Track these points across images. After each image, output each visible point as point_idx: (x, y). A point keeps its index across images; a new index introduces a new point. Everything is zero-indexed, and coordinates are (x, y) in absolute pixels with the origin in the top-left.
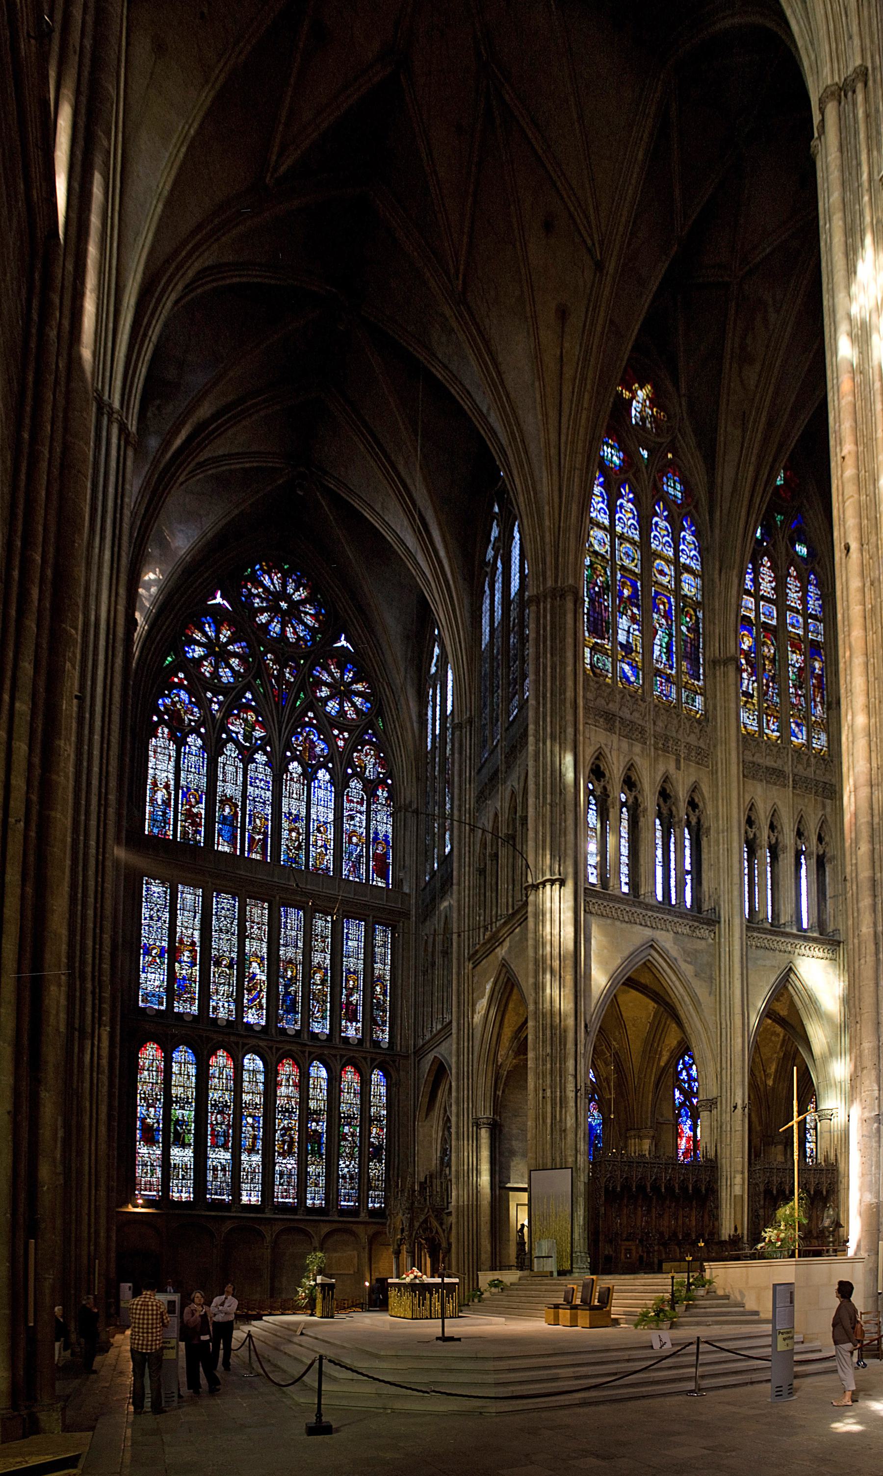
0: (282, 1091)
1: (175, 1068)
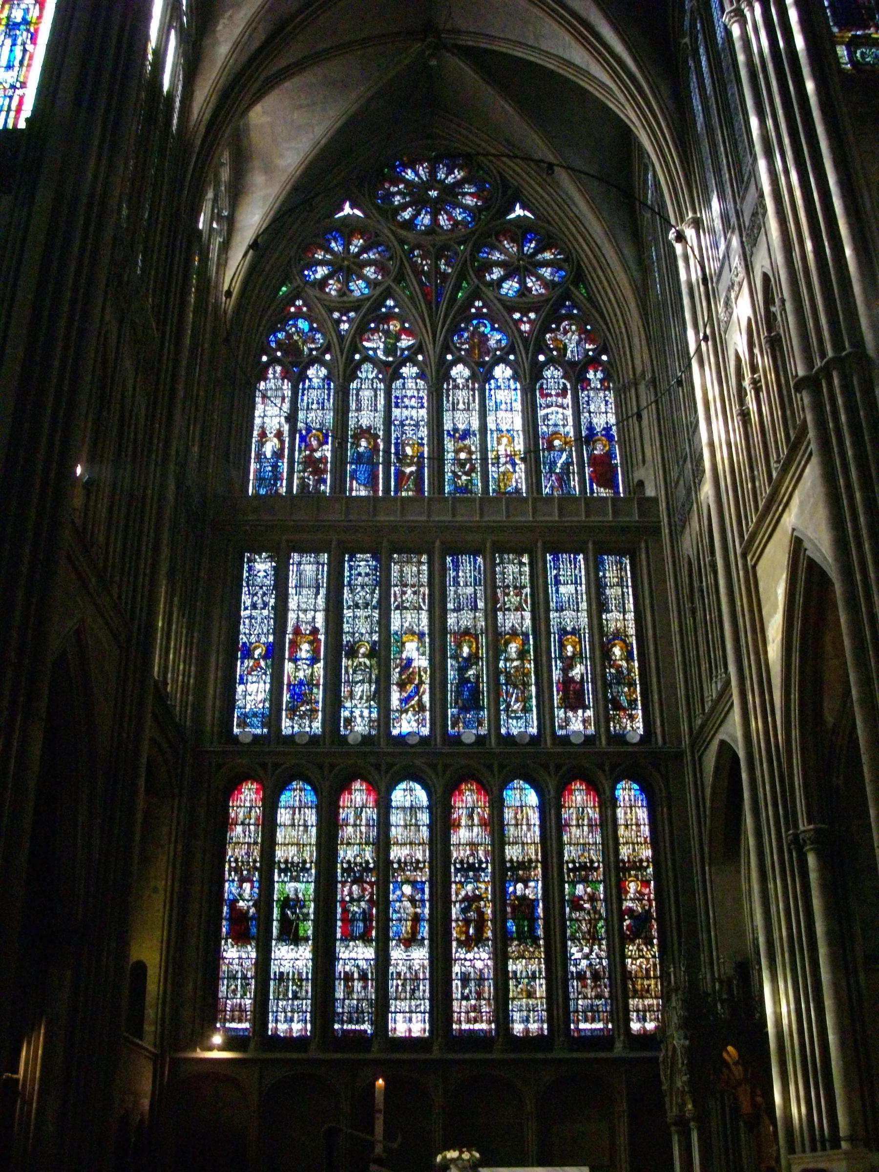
0: (462, 835)
1: (283, 816)
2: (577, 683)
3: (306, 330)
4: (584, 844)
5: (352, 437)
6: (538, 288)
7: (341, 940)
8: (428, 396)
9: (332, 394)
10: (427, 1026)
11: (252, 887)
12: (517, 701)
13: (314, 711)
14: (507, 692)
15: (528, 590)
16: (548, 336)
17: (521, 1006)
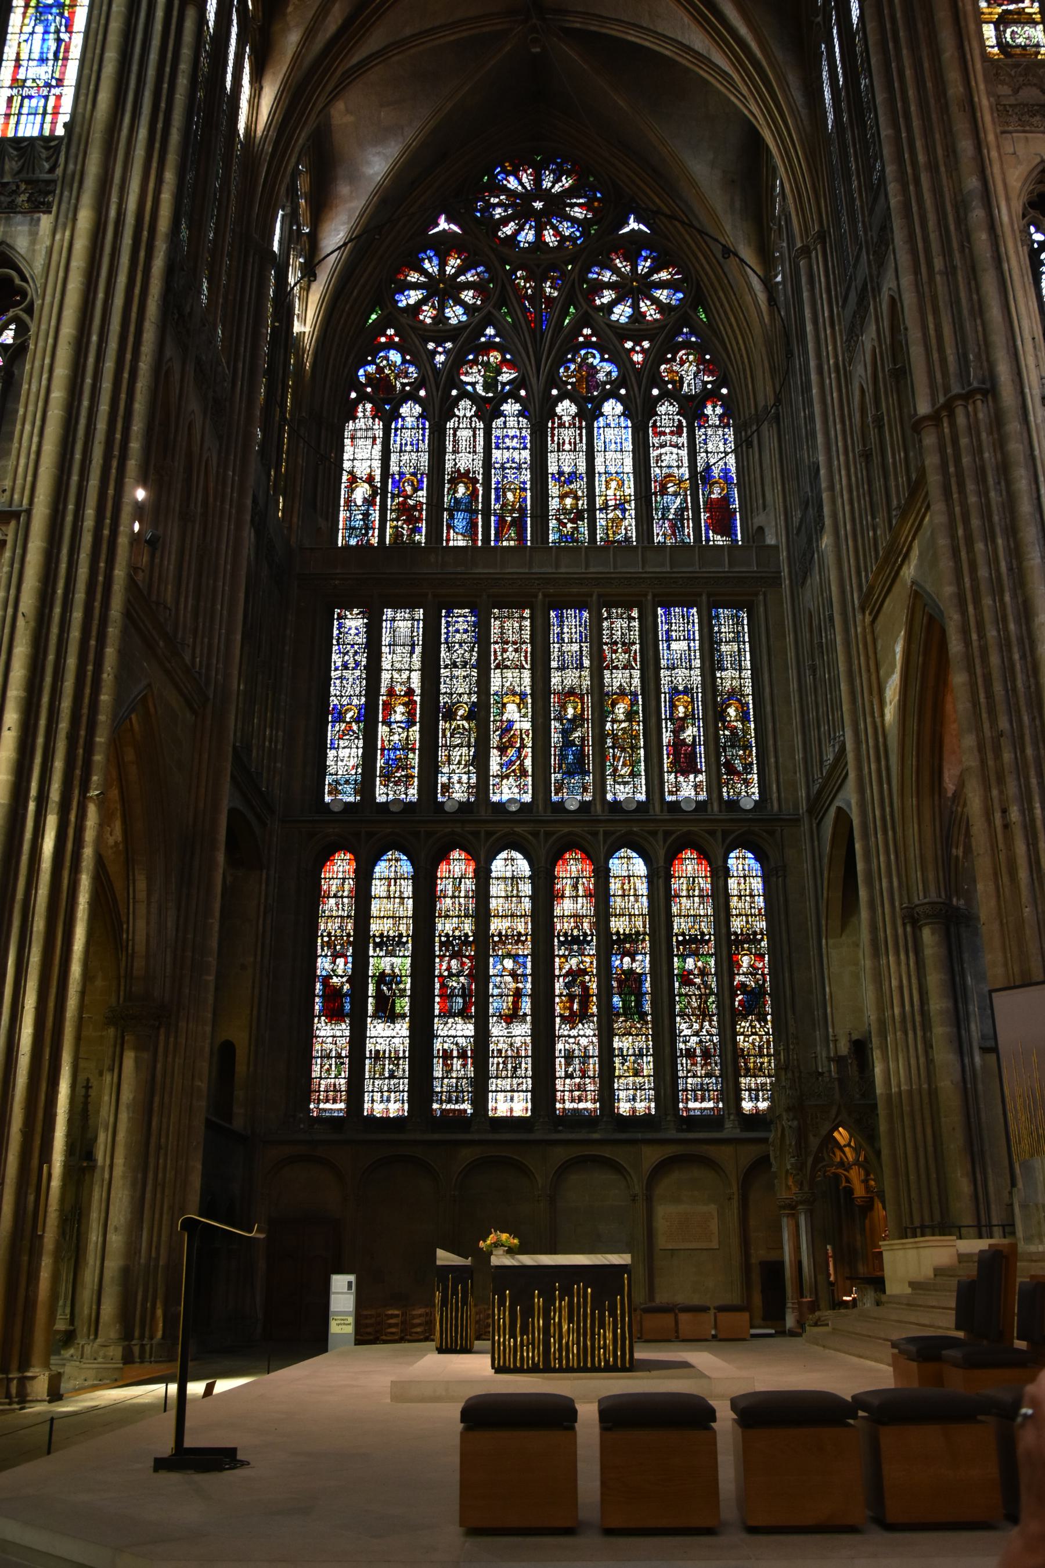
0: (565, 907)
1: (378, 888)
2: (689, 746)
3: (399, 363)
4: (695, 916)
5: (449, 481)
6: (653, 312)
7: (439, 1016)
8: (531, 435)
9: (427, 434)
10: (529, 1105)
11: (346, 963)
12: (624, 765)
13: (410, 777)
14: (614, 756)
15: (638, 646)
16: (663, 367)
17: (627, 1084)
